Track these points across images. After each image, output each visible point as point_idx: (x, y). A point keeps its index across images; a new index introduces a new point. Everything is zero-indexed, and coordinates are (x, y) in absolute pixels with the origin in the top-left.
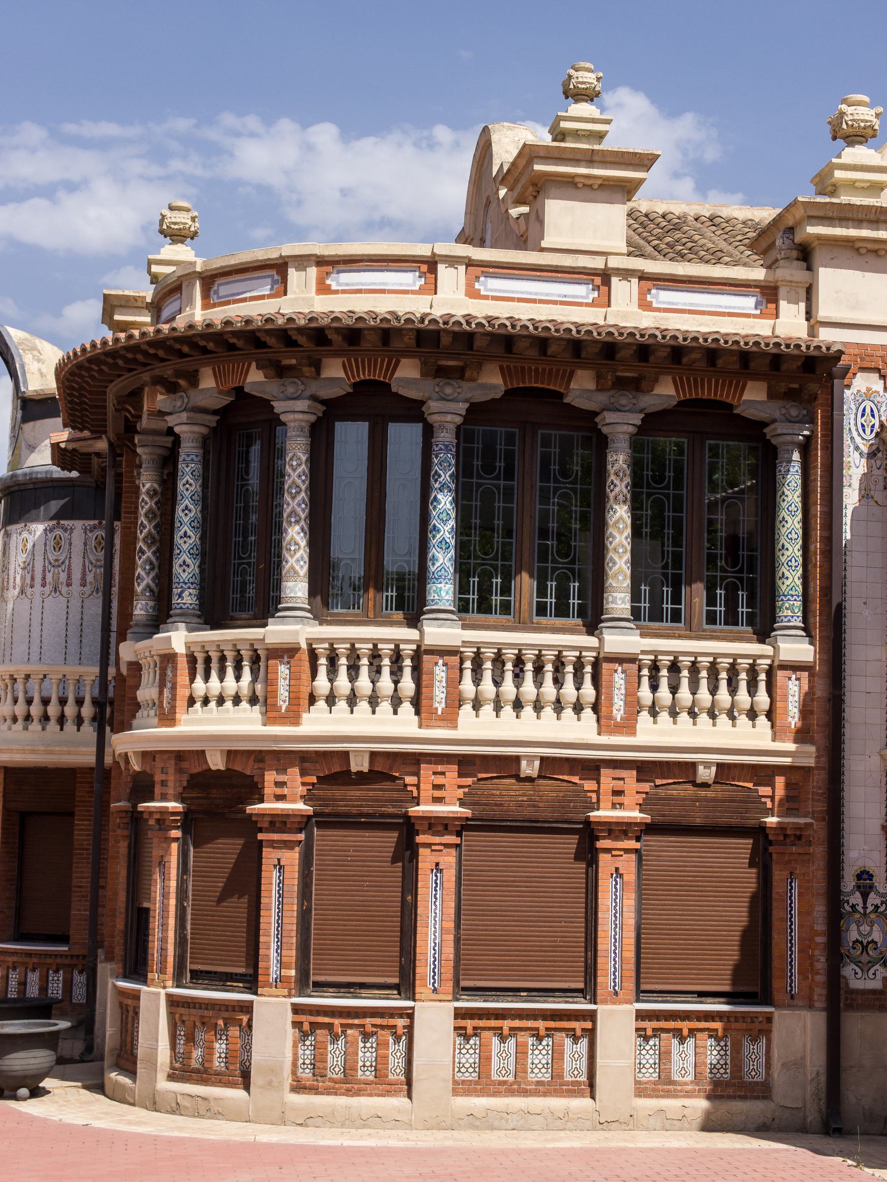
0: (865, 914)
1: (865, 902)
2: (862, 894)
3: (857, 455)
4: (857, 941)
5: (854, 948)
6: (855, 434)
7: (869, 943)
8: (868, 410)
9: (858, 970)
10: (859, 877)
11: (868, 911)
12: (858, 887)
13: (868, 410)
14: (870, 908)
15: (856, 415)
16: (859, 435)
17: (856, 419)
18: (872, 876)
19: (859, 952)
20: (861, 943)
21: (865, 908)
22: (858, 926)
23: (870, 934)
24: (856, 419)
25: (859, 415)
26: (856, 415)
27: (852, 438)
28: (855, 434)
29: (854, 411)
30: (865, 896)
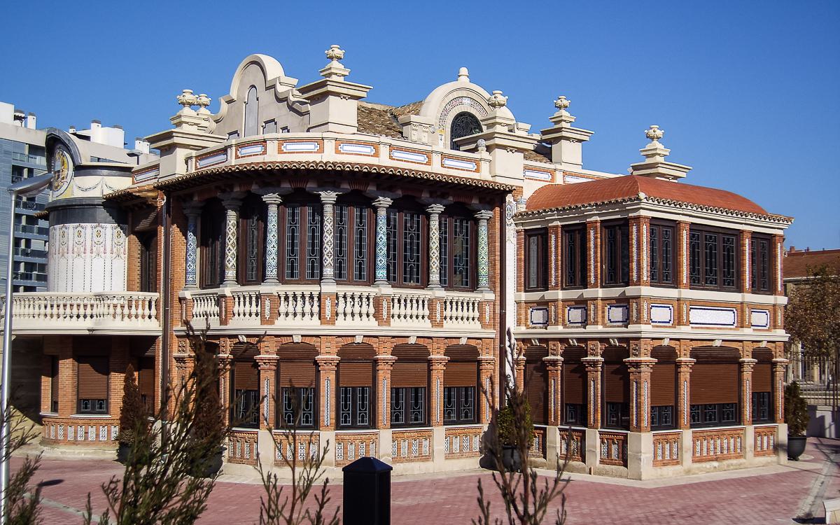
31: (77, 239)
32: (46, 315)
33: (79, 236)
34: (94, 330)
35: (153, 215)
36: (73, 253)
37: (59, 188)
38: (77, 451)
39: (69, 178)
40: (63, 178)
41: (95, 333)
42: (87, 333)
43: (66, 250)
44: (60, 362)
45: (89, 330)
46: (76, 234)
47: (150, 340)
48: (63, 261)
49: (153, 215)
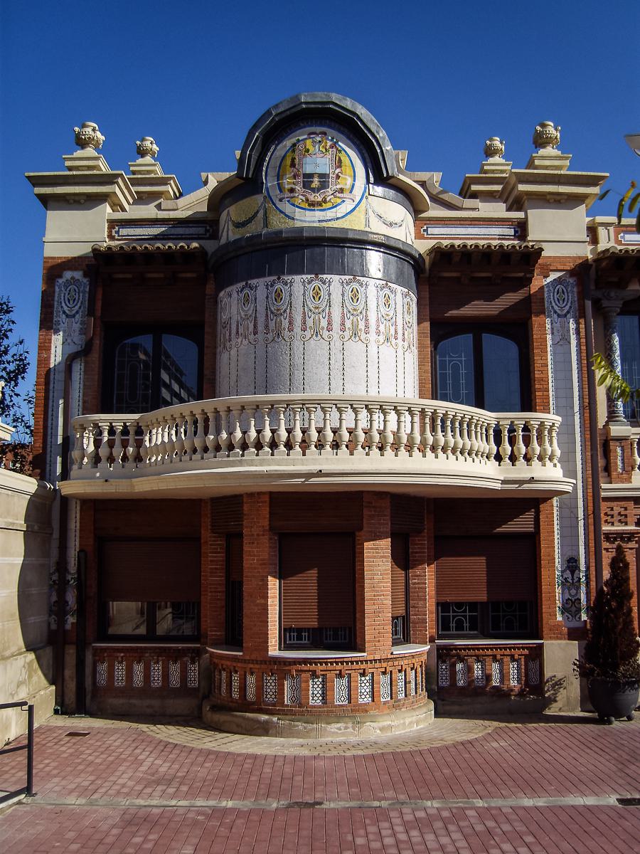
0: (573, 582)
1: (573, 577)
2: (570, 571)
3: (555, 316)
4: (569, 599)
5: (567, 603)
6: (554, 304)
7: (575, 600)
8: (561, 290)
9: (570, 616)
10: (569, 561)
11: (575, 581)
12: (568, 567)
13: (561, 290)
14: (576, 580)
15: (554, 293)
16: (556, 304)
17: (554, 296)
18: (576, 560)
19: (570, 606)
20: (571, 600)
21: (573, 579)
22: (569, 591)
23: (576, 594)
24: (554, 296)
25: (556, 294)
26: (554, 293)
27: (552, 307)
28: (554, 304)
29: (552, 291)
30: (573, 573)
31: (383, 310)
32: (206, 449)
33: (387, 304)
34: (532, 480)
35: (509, 299)
36: (378, 333)
37: (325, 206)
38: (407, 721)
39: (358, 192)
40: (342, 191)
41: (526, 486)
42: (498, 486)
43: (362, 325)
44: (366, 544)
45: (504, 482)
46: (382, 300)
47: (530, 502)
48: (355, 348)
49: (509, 299)
